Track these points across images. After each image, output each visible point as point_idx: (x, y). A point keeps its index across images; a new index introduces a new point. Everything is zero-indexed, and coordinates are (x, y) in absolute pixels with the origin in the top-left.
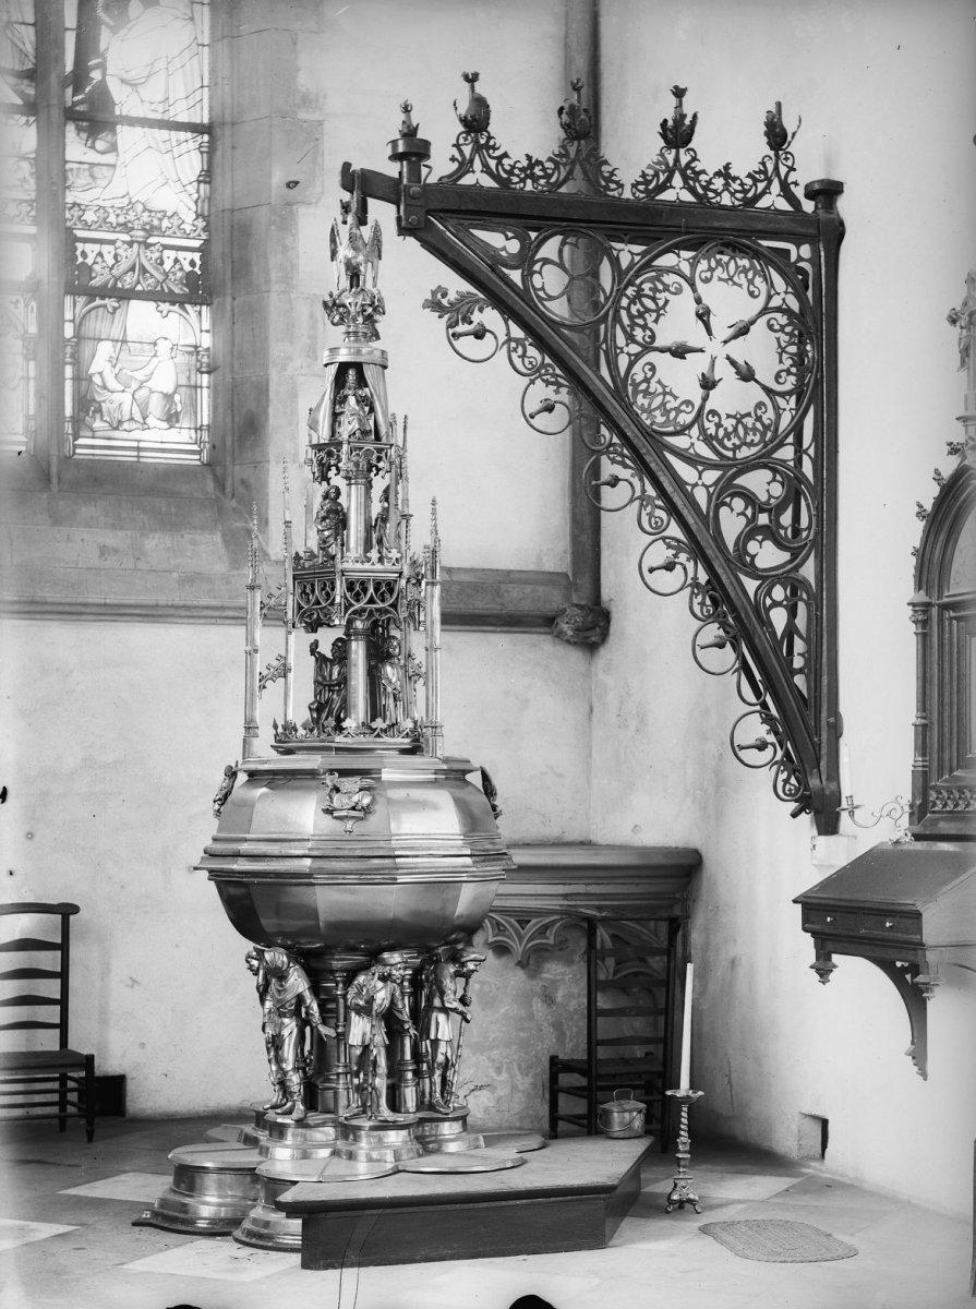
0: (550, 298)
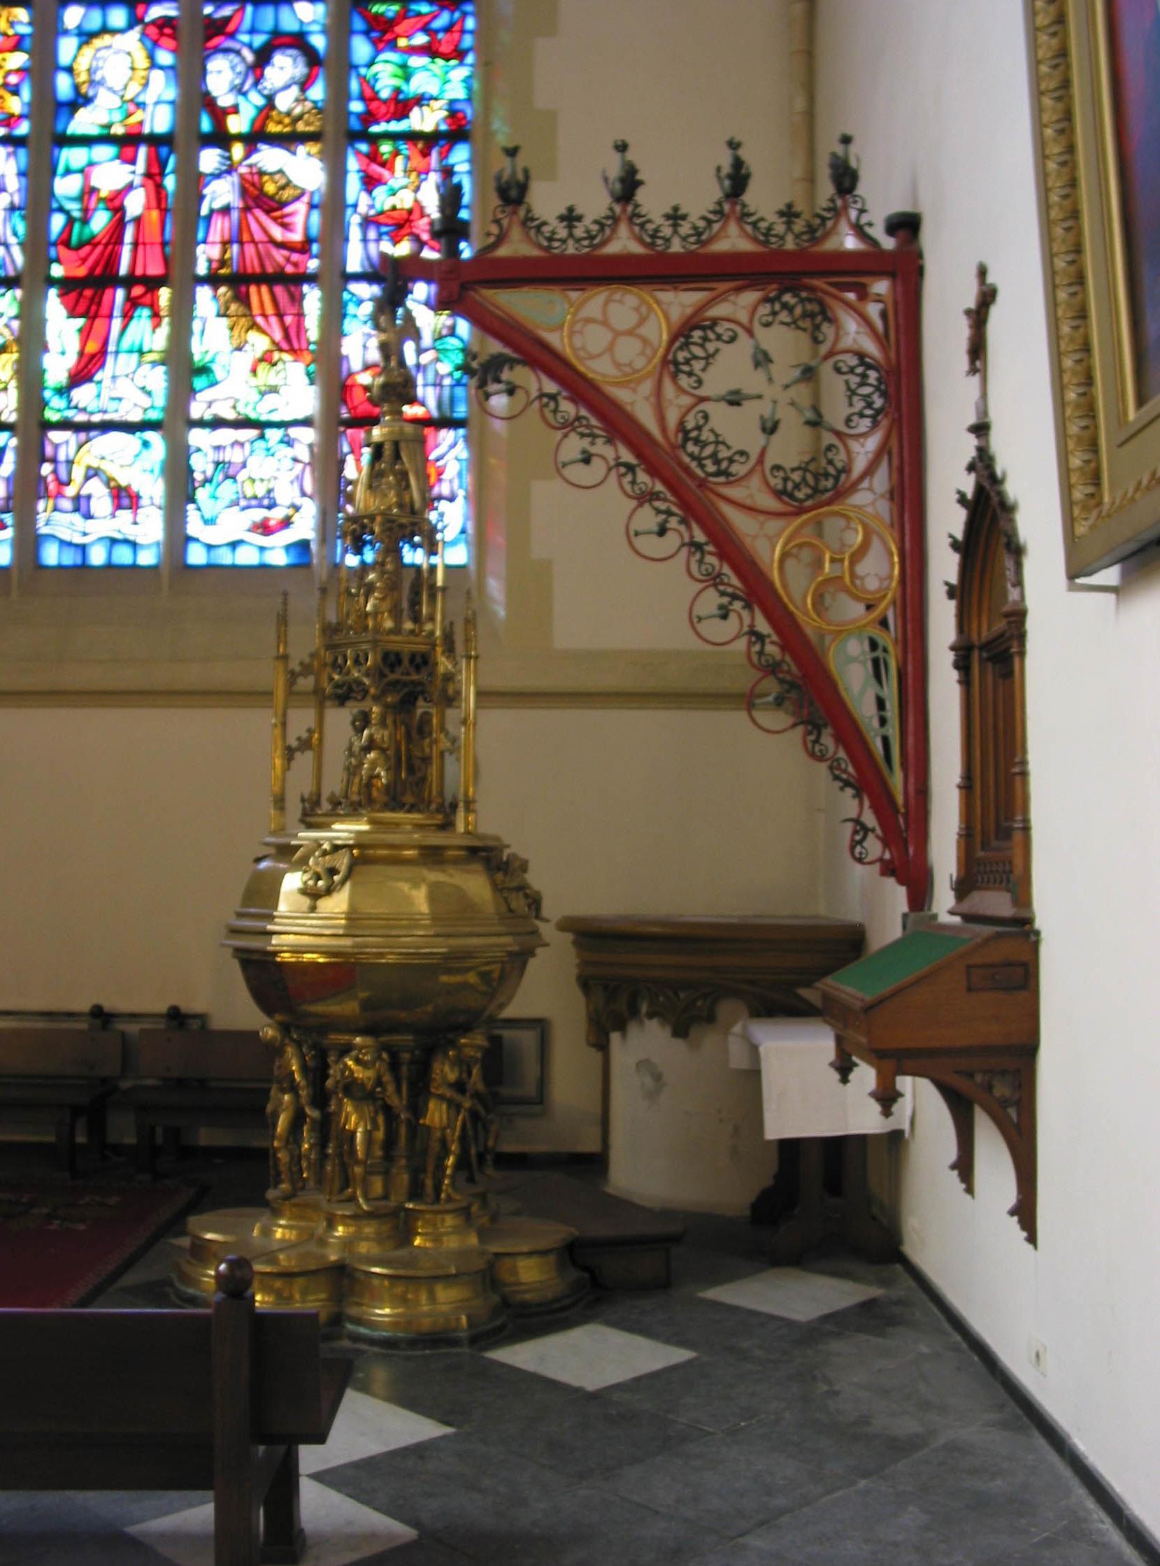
0: (592, 357)
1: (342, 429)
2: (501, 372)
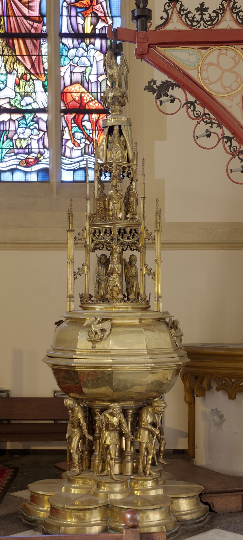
0: (212, 83)
1: (62, 114)
2: (168, 91)
